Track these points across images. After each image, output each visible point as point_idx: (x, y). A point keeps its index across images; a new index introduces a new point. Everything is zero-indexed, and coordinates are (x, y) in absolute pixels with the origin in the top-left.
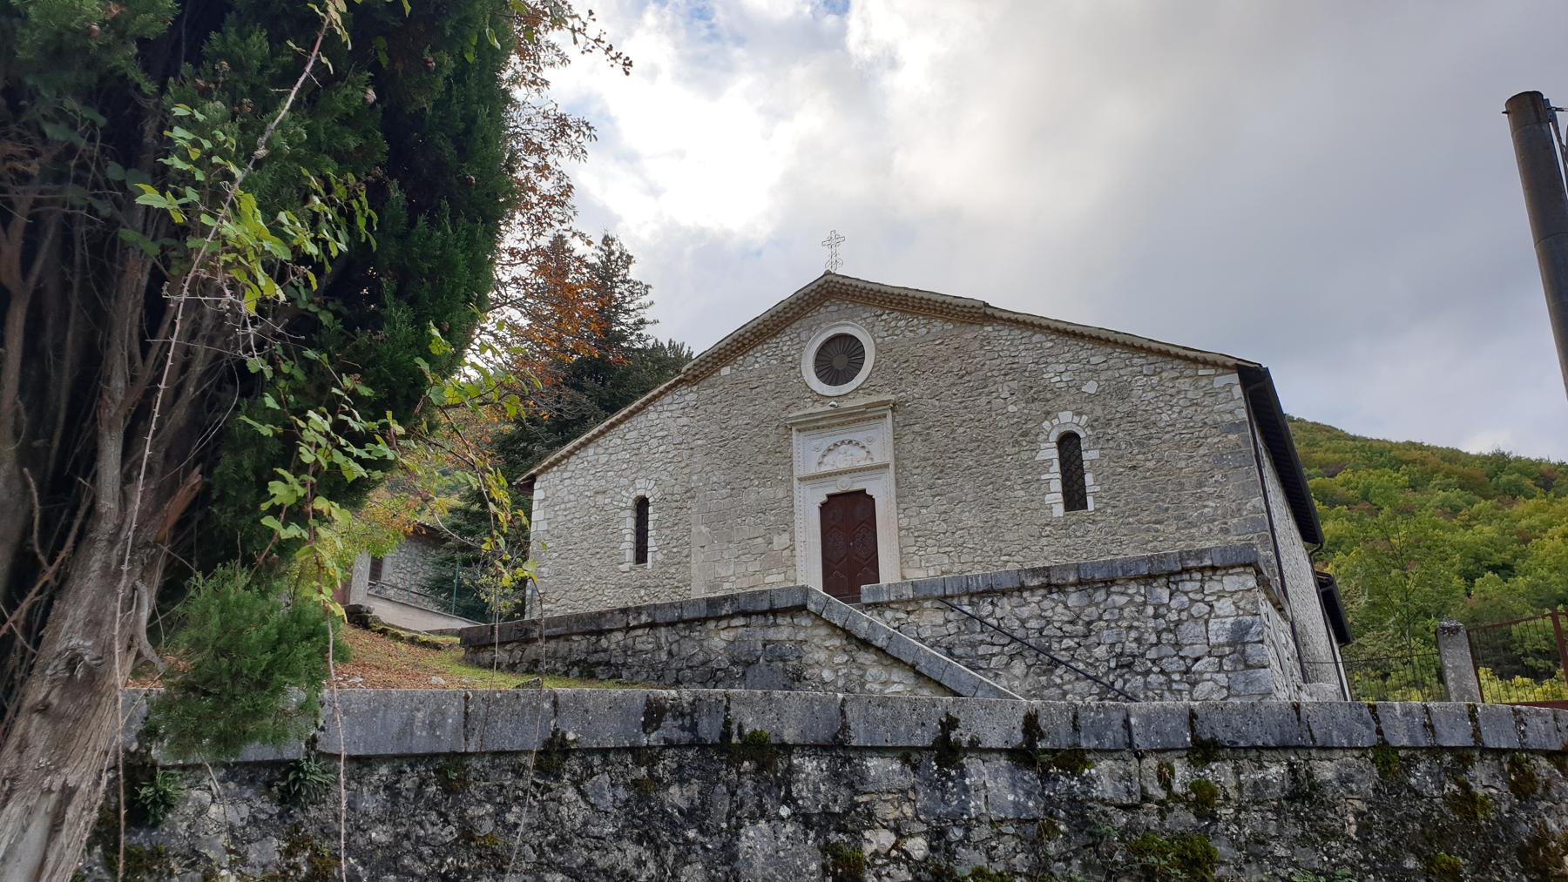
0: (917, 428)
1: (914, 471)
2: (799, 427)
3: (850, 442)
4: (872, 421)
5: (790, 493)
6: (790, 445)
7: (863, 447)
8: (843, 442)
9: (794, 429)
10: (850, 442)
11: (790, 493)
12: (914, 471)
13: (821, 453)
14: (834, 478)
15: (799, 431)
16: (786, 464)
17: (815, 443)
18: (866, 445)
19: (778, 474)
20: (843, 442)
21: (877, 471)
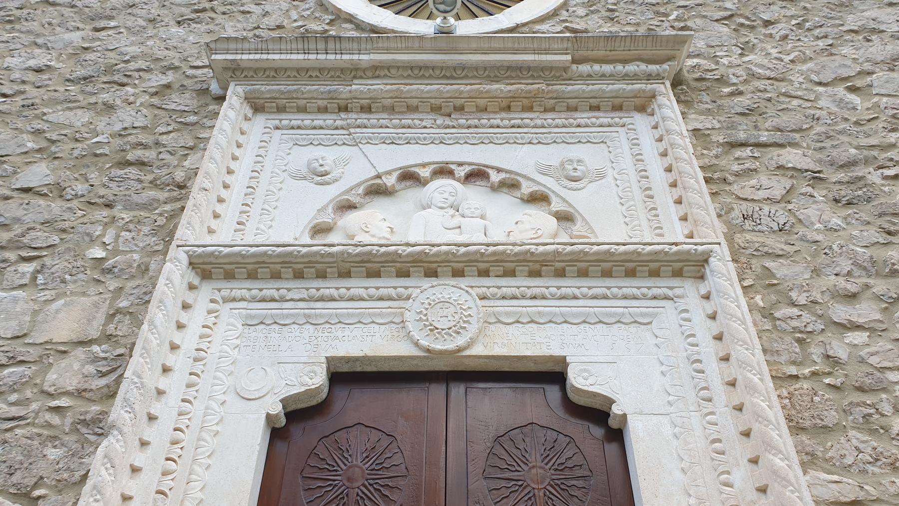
0: (791, 157)
1: (841, 312)
2: (264, 88)
3: (477, 175)
4: (583, 117)
5: (122, 327)
6: (198, 145)
7: (538, 199)
8: (443, 171)
9: (235, 94)
10: (477, 175)
11: (122, 327)
12: (841, 312)
13: (332, 192)
14: (387, 285)
15: (257, 106)
16: (147, 206)
17: (329, 155)
18: (549, 183)
19: (93, 240)
20: (443, 171)
21: (630, 286)
